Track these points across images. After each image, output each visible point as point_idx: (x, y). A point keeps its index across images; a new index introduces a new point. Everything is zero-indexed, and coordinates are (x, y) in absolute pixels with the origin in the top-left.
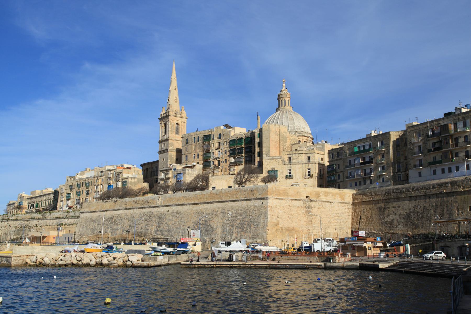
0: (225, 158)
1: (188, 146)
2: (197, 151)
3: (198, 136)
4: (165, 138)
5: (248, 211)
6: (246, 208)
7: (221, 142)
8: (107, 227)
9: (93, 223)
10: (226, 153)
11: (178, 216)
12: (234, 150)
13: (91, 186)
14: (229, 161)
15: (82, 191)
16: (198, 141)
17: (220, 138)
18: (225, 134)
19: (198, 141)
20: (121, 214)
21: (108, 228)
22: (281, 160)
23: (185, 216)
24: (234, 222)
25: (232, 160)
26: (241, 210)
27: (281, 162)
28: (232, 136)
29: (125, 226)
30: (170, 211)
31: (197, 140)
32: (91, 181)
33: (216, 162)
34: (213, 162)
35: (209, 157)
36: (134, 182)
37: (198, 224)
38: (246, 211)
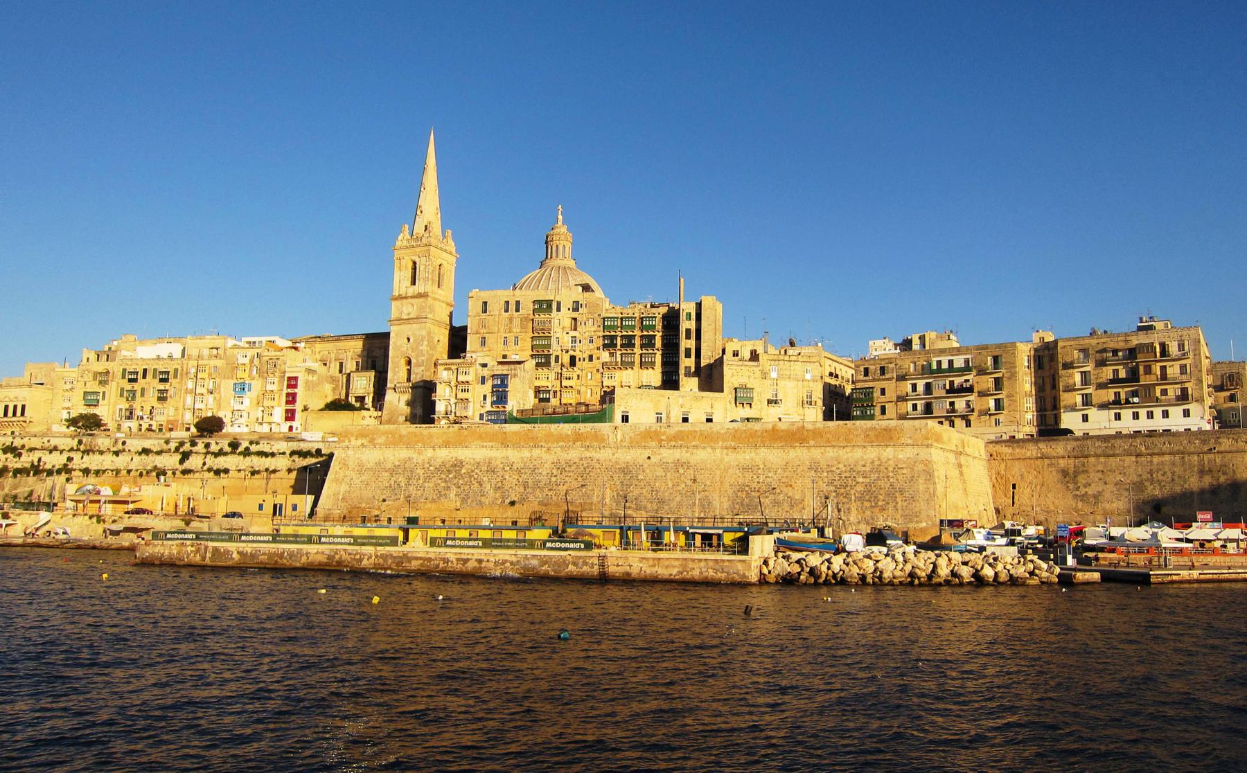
0: (589, 353)
2: (515, 330)
3: (518, 299)
4: (412, 291)
5: (882, 468)
6: (877, 463)
7: (579, 319)
8: (443, 485)
10: (591, 341)
11: (681, 471)
12: (613, 338)
14: (598, 358)
15: (143, 390)
16: (517, 310)
17: (576, 309)
18: (590, 303)
19: (517, 310)
20: (490, 459)
21: (448, 488)
22: (759, 368)
23: (703, 471)
24: (849, 488)
25: (605, 356)
26: (864, 466)
27: (758, 374)
28: (607, 310)
30: (653, 459)
31: (512, 307)
32: (176, 370)
33: (566, 359)
34: (557, 357)
35: (549, 346)
36: (312, 382)
37: (747, 488)
38: (879, 467)
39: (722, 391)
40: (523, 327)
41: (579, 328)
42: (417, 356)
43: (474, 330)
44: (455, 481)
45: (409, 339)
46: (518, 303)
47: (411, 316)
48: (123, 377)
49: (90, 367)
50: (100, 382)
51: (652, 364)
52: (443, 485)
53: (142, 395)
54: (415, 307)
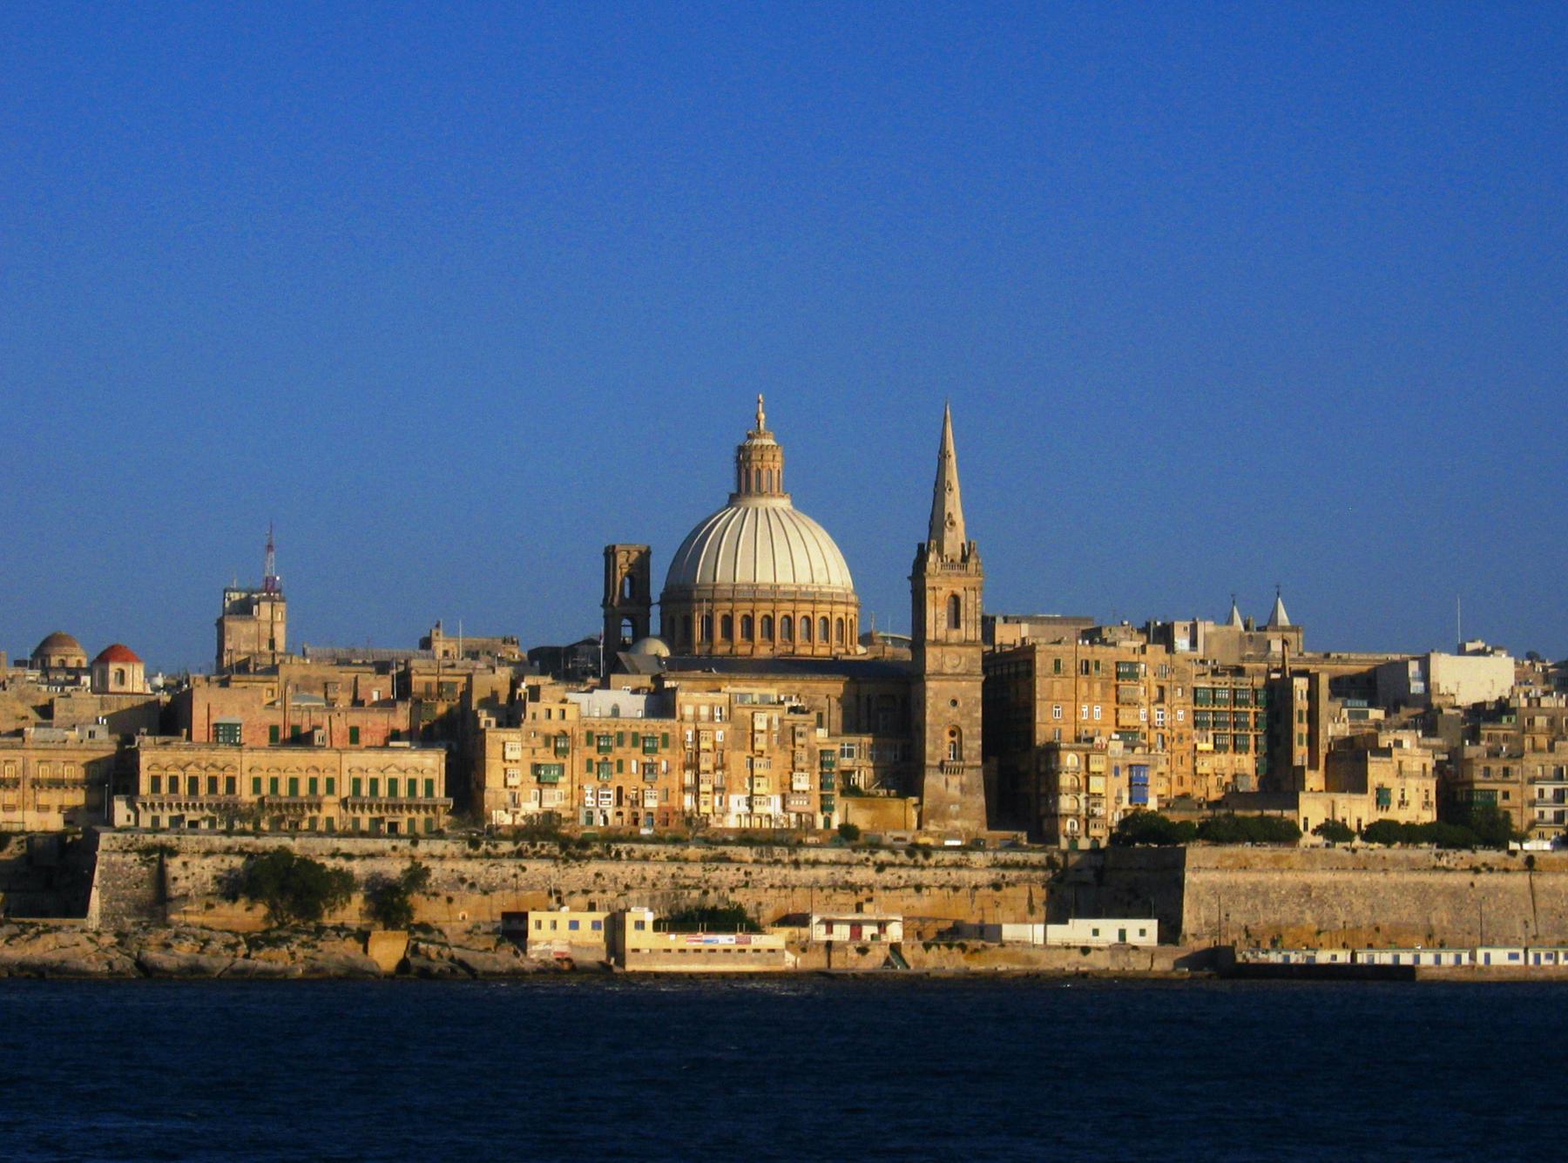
0: (1177, 730)
1: (1063, 680)
3: (1097, 658)
7: (1166, 685)
9: (1243, 898)
13: (664, 751)
20: (1335, 882)
21: (1302, 912)
29: (1355, 910)
39: (1366, 792)
40: (1104, 694)
41: (1167, 700)
42: (969, 726)
43: (1044, 695)
44: (1308, 905)
45: (954, 703)
46: (1097, 663)
47: (958, 670)
48: (589, 742)
49: (537, 727)
50: (556, 751)
51: (1246, 749)
52: (1298, 908)
53: (620, 770)
54: (963, 659)
